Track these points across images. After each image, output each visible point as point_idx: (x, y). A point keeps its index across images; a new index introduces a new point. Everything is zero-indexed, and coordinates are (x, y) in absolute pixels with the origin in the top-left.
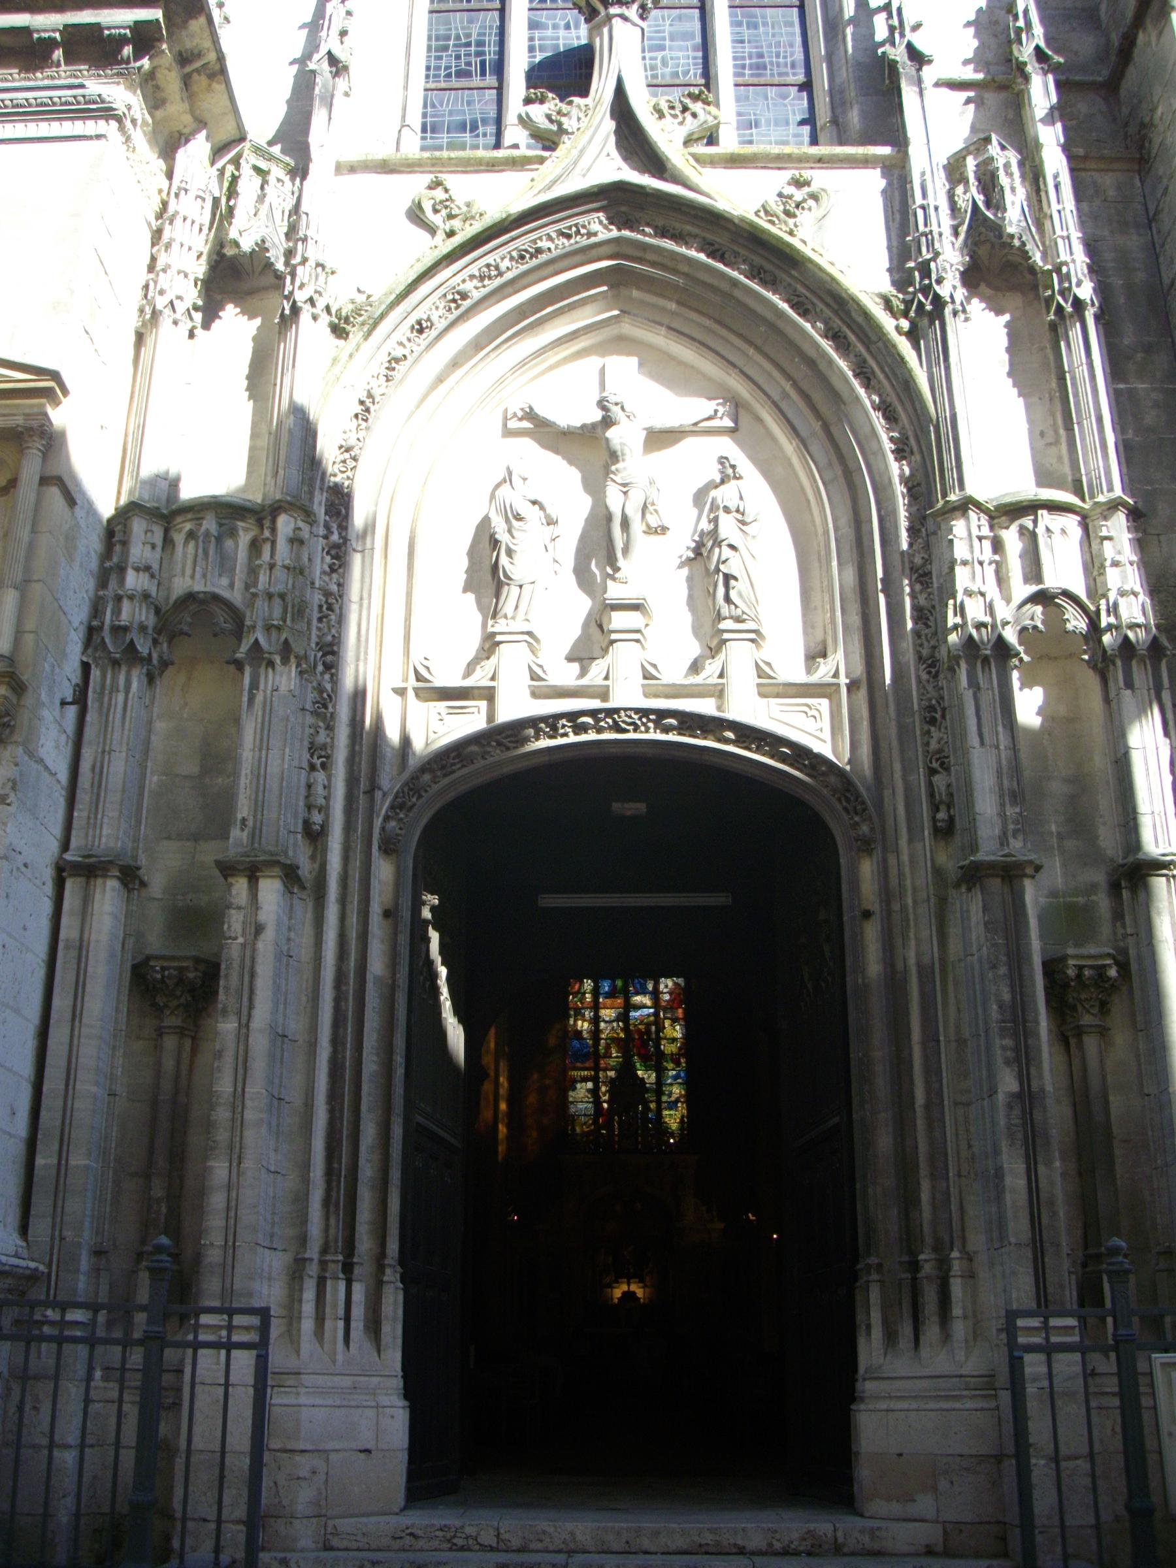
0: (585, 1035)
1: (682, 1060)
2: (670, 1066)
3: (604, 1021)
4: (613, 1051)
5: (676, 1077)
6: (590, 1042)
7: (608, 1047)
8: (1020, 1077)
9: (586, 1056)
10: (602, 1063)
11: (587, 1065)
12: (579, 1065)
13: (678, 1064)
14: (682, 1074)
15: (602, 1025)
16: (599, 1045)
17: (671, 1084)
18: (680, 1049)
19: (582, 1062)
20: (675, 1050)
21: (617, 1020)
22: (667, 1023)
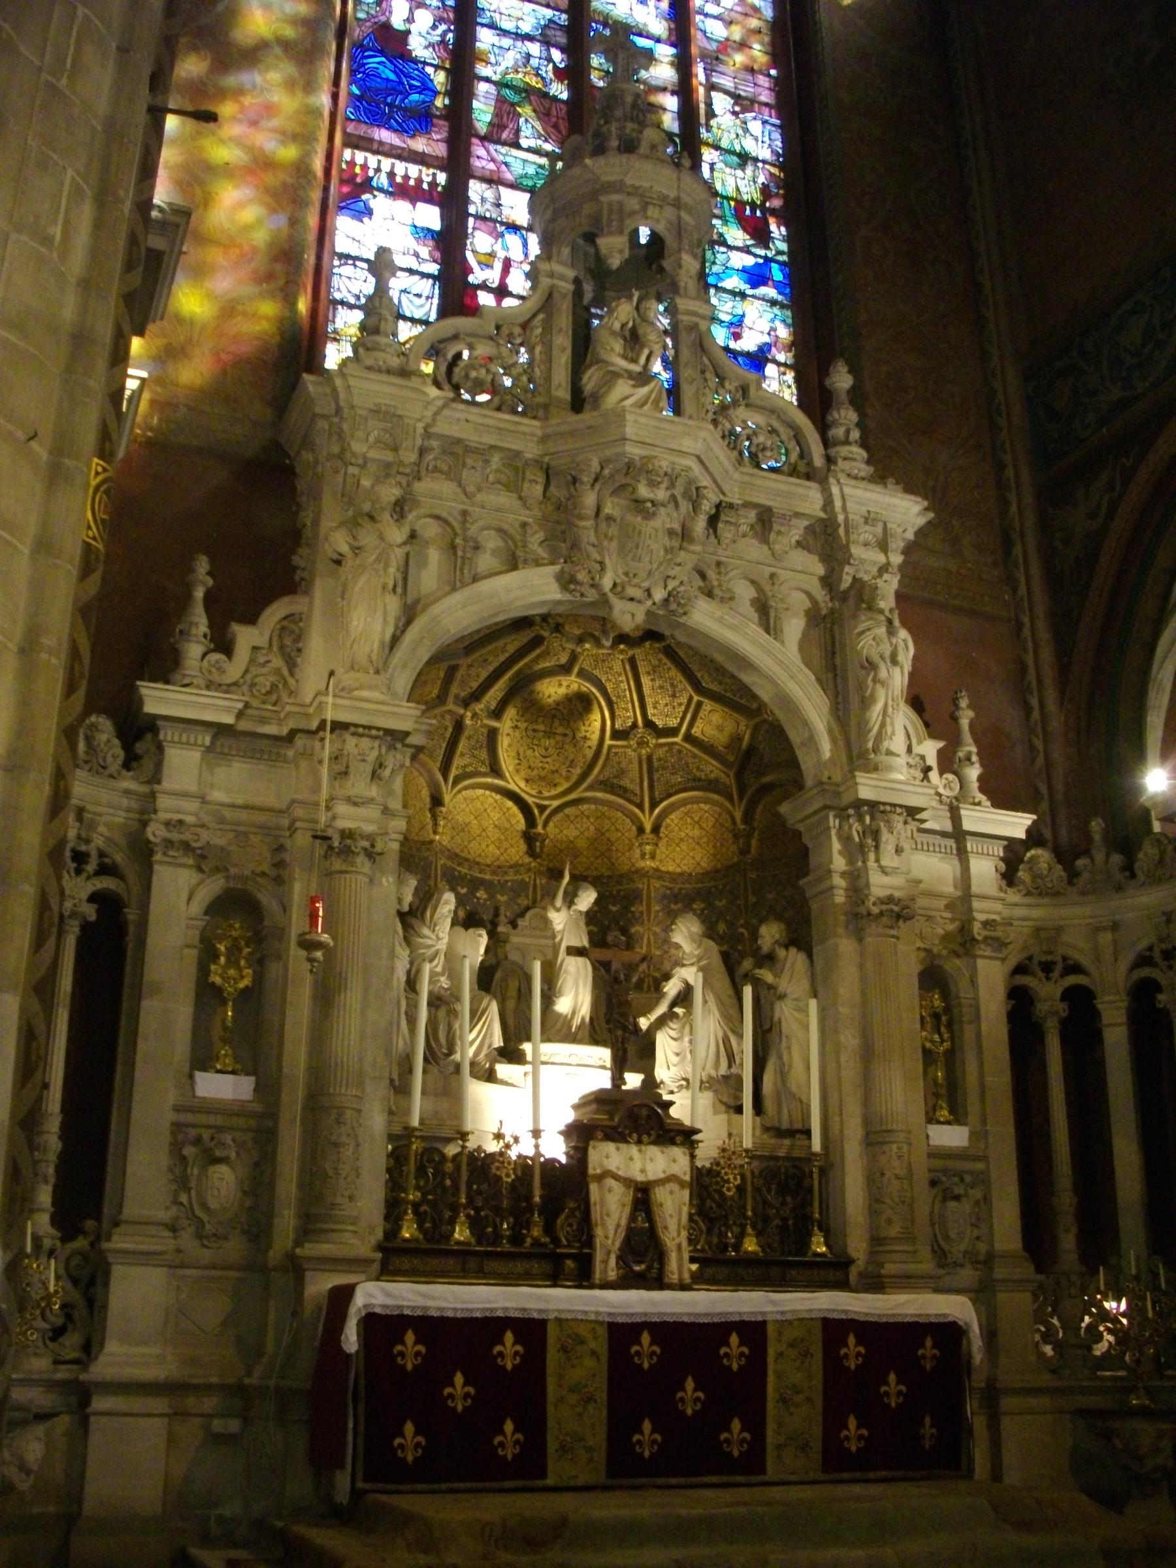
0: (418, 46)
1: (777, 230)
2: (736, 235)
3: (492, 26)
4: (526, 130)
5: (757, 277)
6: (439, 79)
7: (505, 113)
8: (613, 1079)
9: (421, 120)
10: (482, 157)
11: (419, 144)
12: (385, 135)
13: (761, 236)
14: (777, 274)
15: (485, 38)
16: (471, 95)
17: (743, 295)
18: (765, 191)
19: (401, 130)
20: (750, 193)
21: (544, 37)
22: (721, 103)
